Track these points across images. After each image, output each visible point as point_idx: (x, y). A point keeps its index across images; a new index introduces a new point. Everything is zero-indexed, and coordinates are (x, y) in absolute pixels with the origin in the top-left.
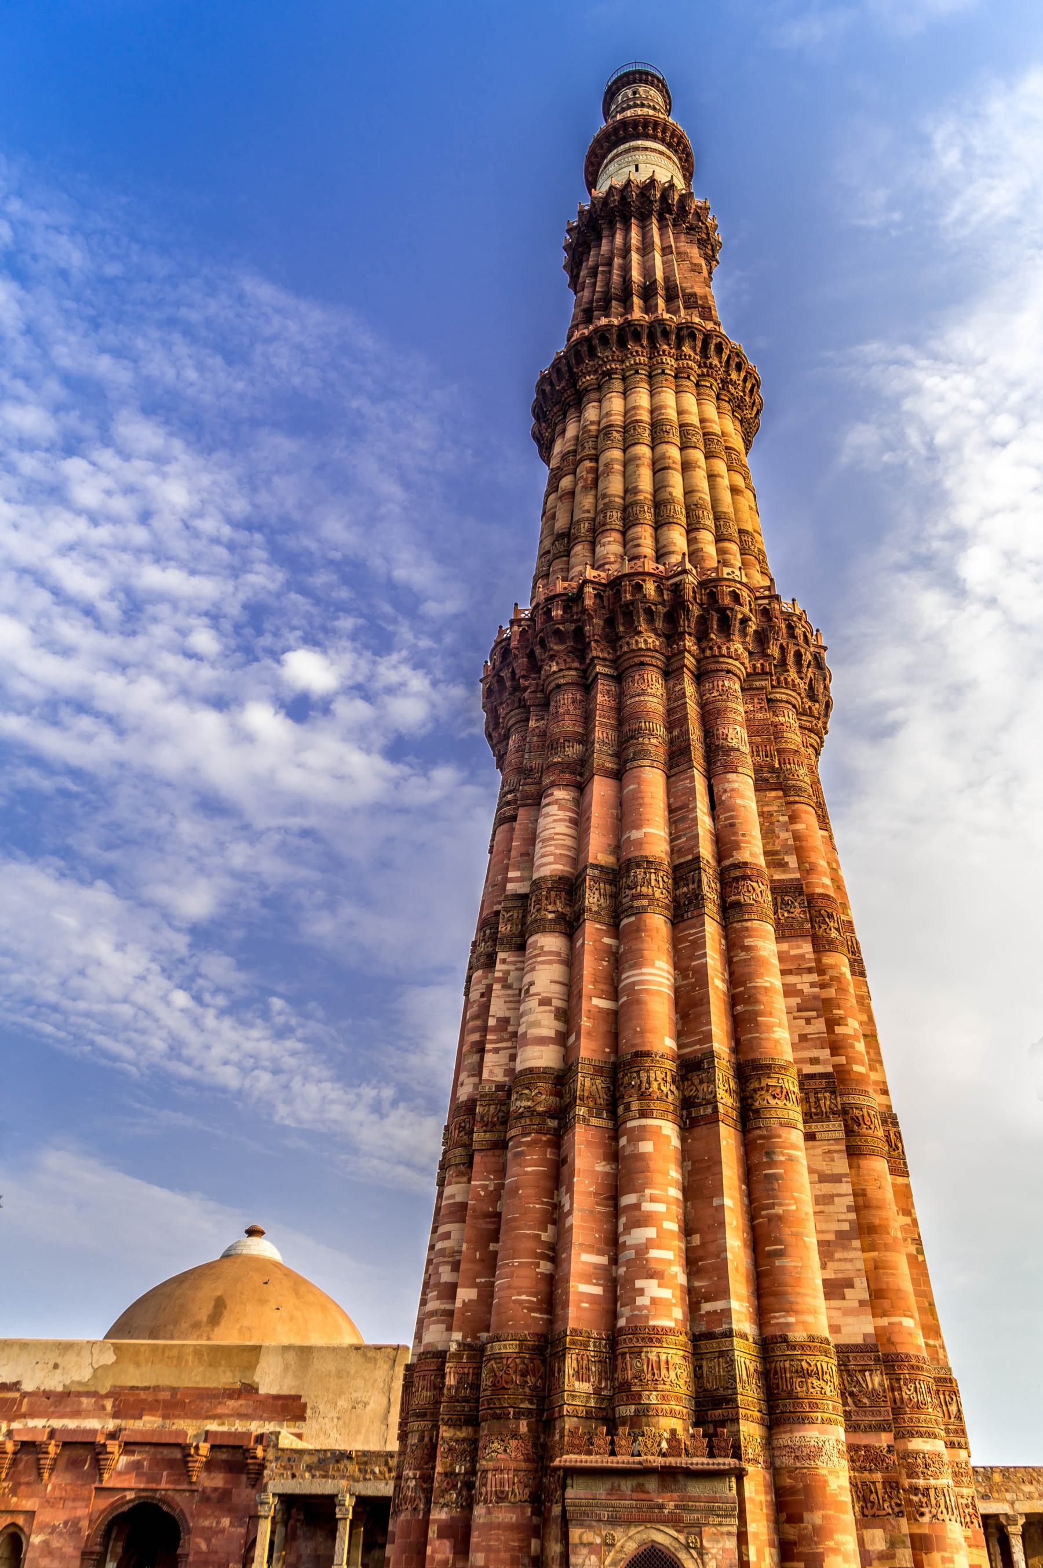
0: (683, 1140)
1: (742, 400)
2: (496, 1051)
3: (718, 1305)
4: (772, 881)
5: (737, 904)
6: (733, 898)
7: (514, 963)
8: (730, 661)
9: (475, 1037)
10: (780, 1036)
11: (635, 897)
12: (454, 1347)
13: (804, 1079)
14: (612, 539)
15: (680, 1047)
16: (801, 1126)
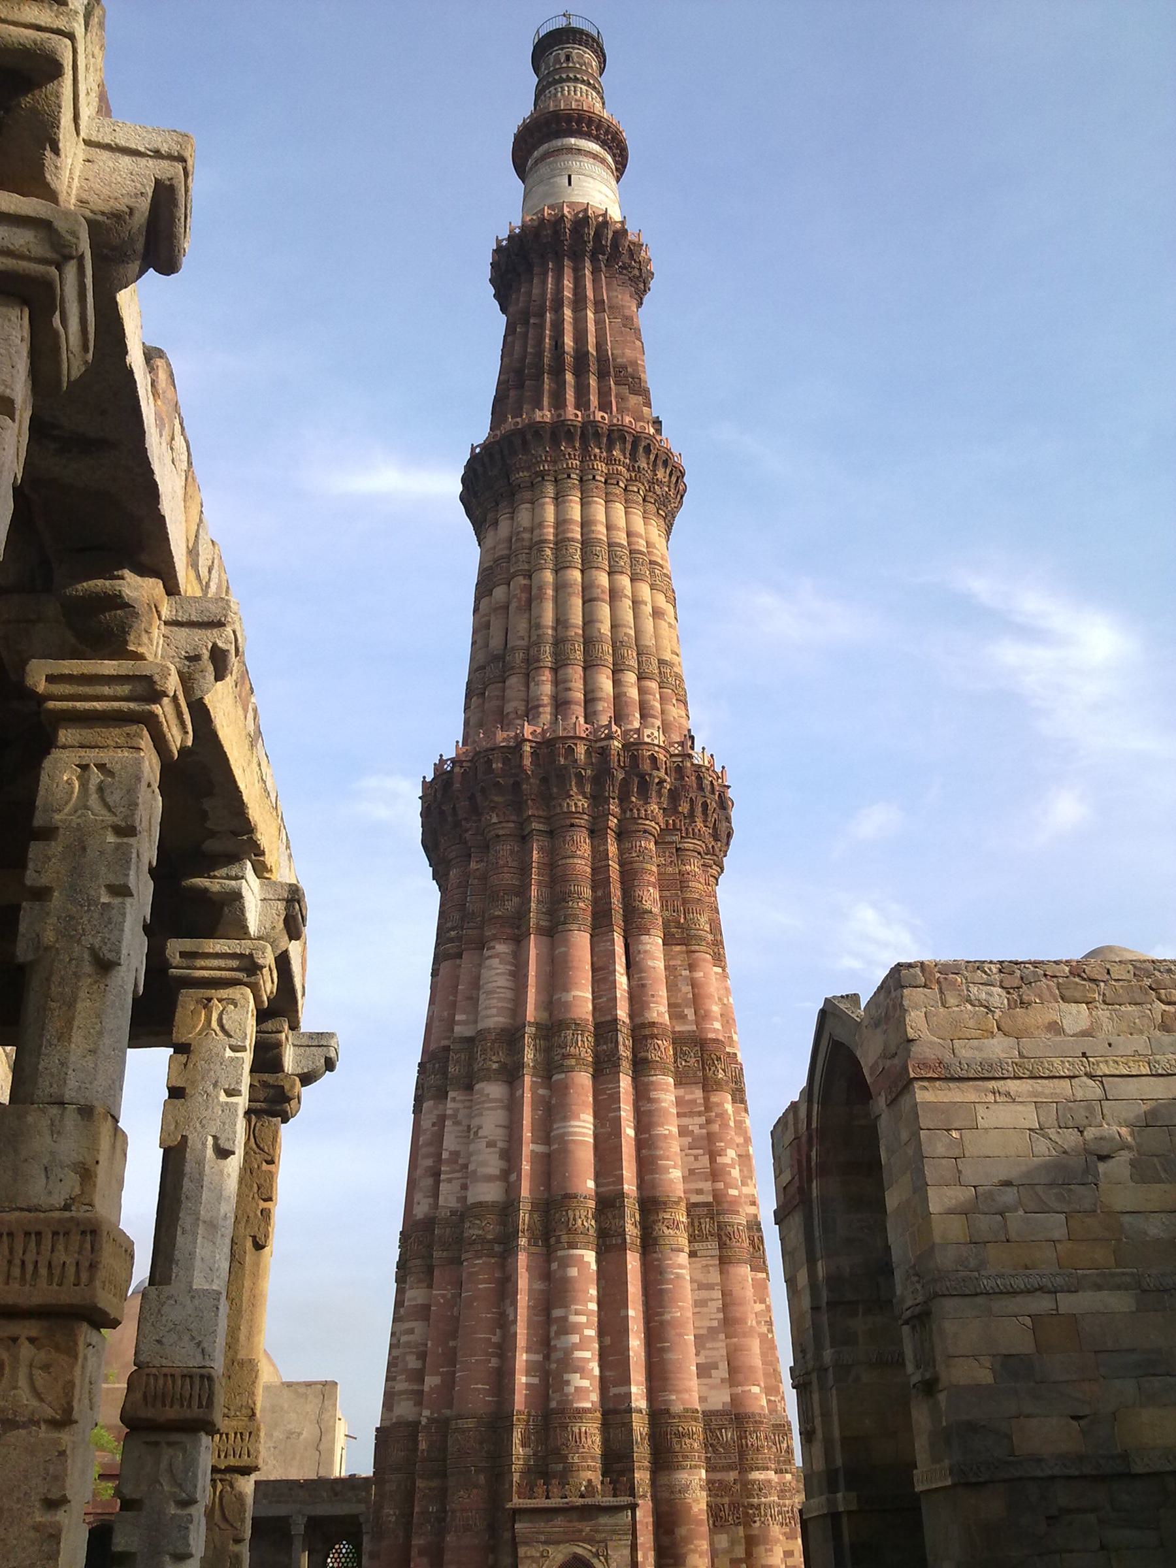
0: (598, 1261)
2: (449, 1181)
3: (621, 1390)
4: (674, 1032)
6: (642, 1054)
8: (647, 822)
10: (674, 1176)
12: (424, 1421)
13: (691, 1208)
15: (597, 1185)
16: (687, 1250)
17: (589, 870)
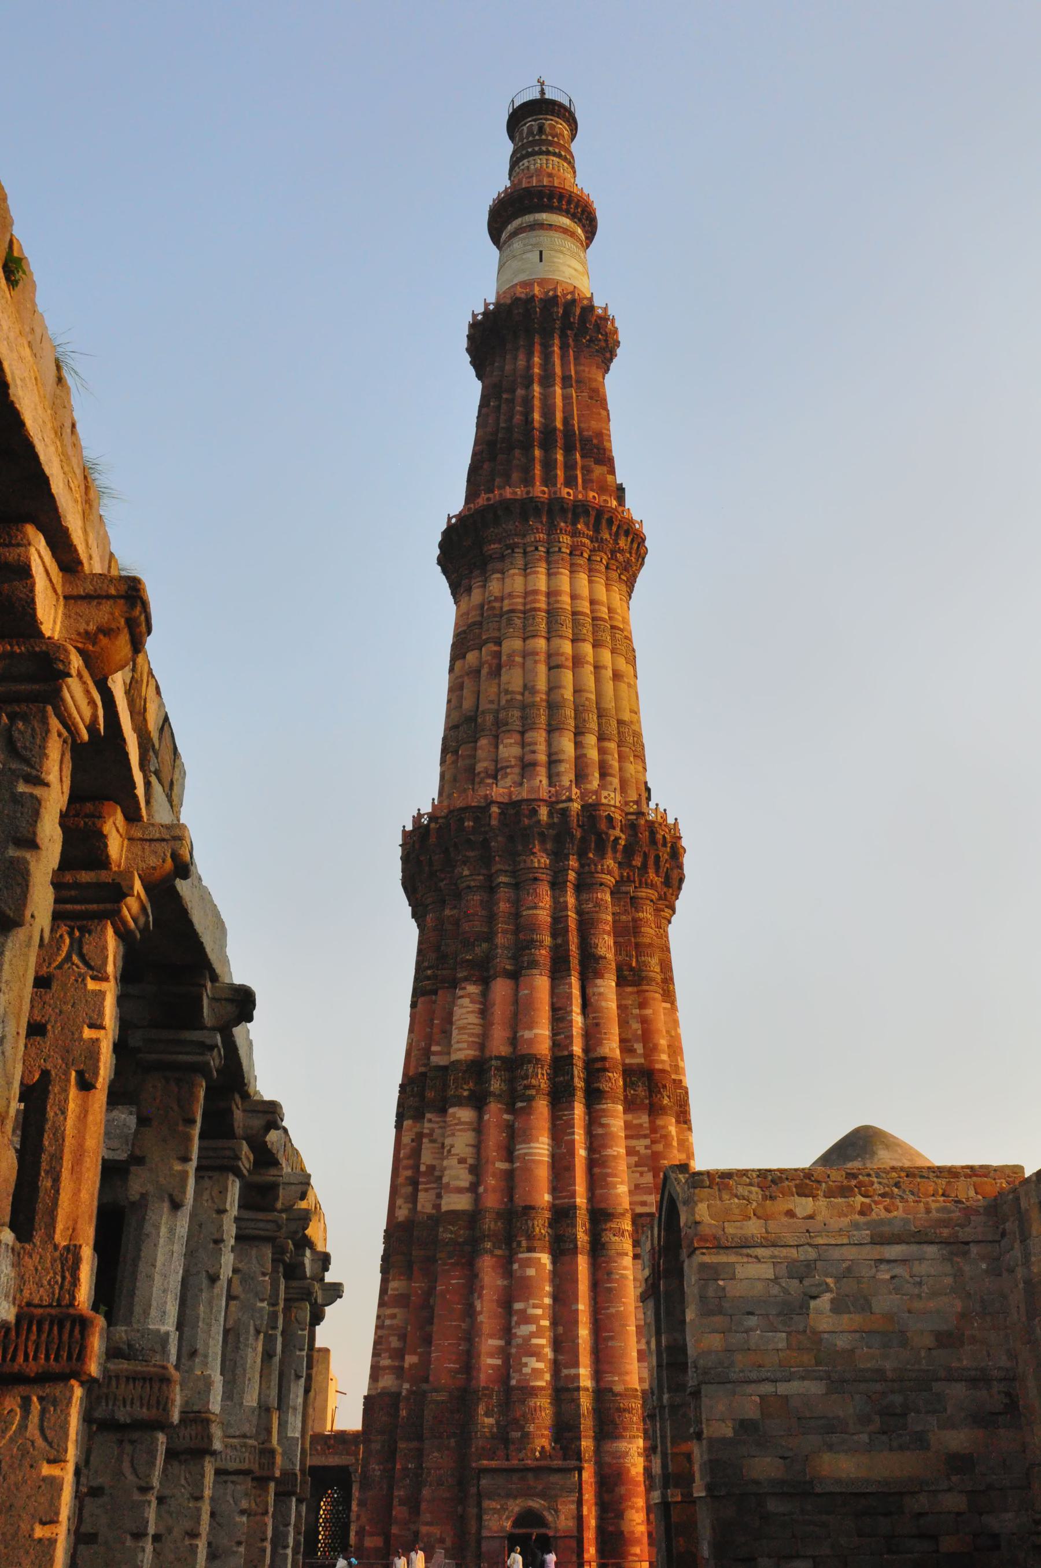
0: (554, 1262)
1: (628, 561)
2: (426, 1190)
6: (596, 1085)
7: (437, 1122)
8: (604, 876)
9: (409, 1173)
12: (404, 1393)
13: (636, 1218)
14: (512, 741)
15: (554, 1198)
16: (631, 1254)
17: (549, 919)
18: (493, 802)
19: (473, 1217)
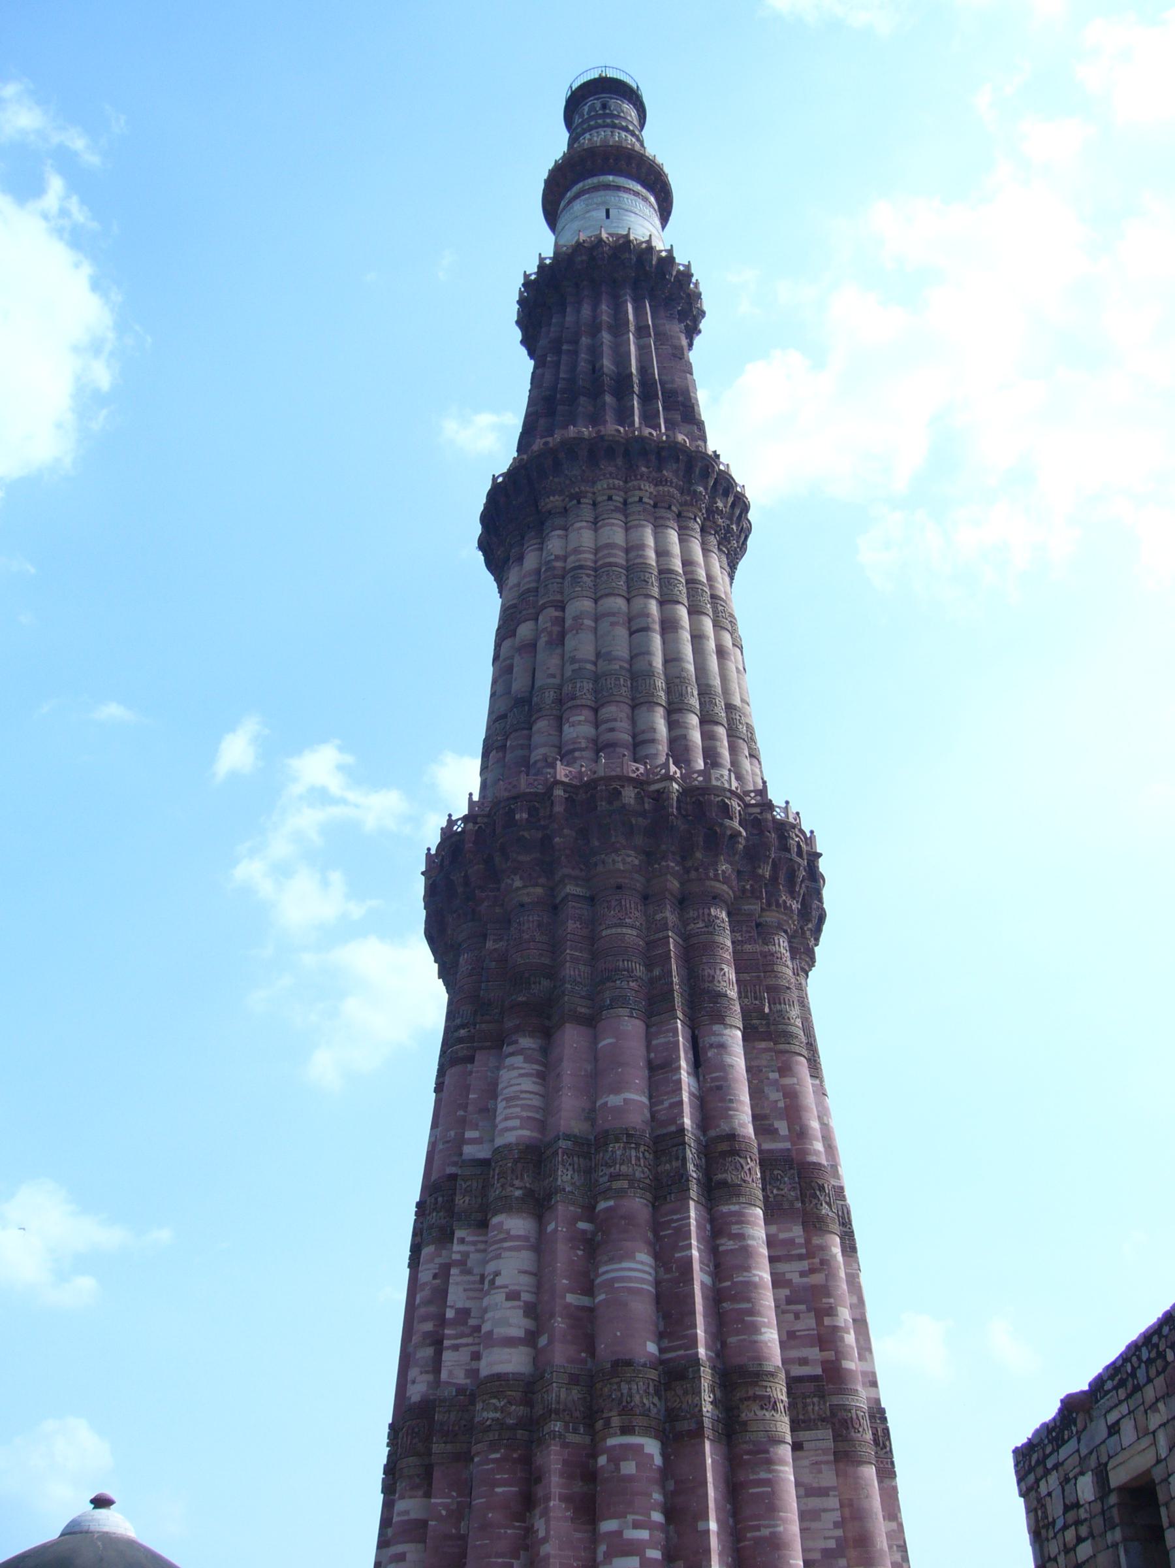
0: (665, 1455)
1: (728, 530)
2: (456, 1348)
5: (724, 1184)
6: (720, 1176)
7: (474, 1243)
8: (718, 885)
11: (614, 1177)
13: (793, 1383)
14: (582, 718)
15: (661, 1350)
16: (789, 1439)
18: (557, 782)
19: (530, 1387)
